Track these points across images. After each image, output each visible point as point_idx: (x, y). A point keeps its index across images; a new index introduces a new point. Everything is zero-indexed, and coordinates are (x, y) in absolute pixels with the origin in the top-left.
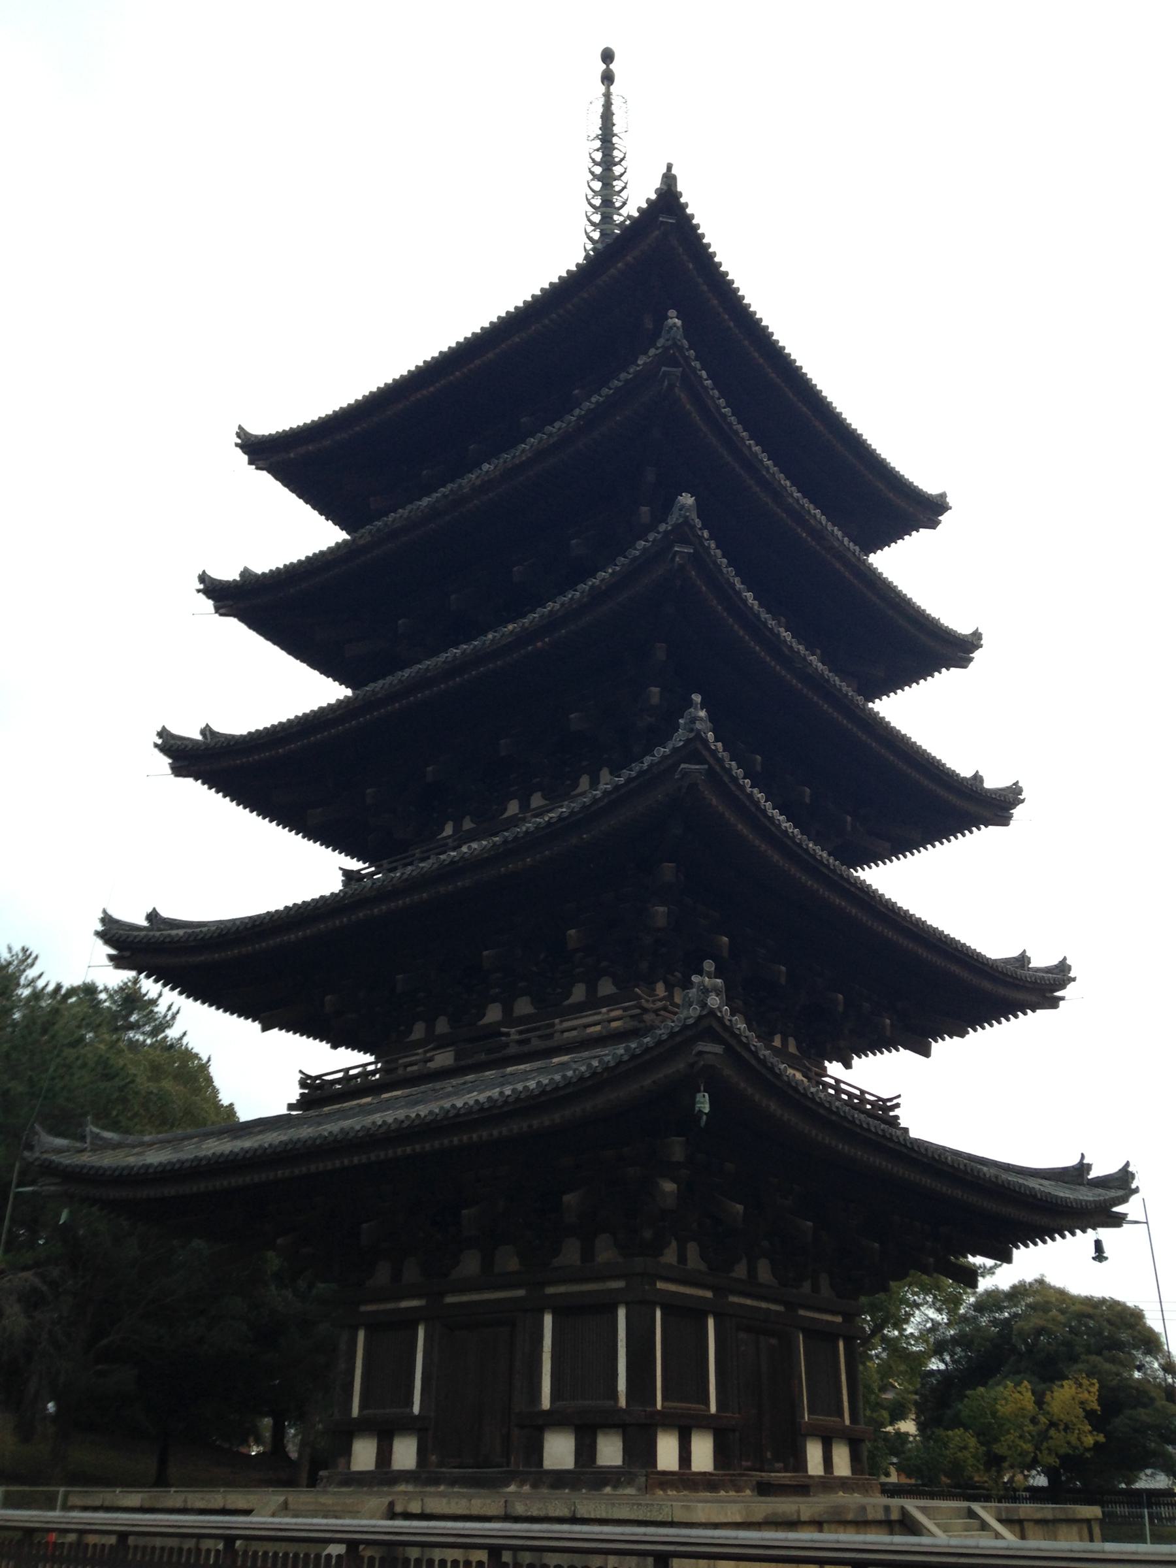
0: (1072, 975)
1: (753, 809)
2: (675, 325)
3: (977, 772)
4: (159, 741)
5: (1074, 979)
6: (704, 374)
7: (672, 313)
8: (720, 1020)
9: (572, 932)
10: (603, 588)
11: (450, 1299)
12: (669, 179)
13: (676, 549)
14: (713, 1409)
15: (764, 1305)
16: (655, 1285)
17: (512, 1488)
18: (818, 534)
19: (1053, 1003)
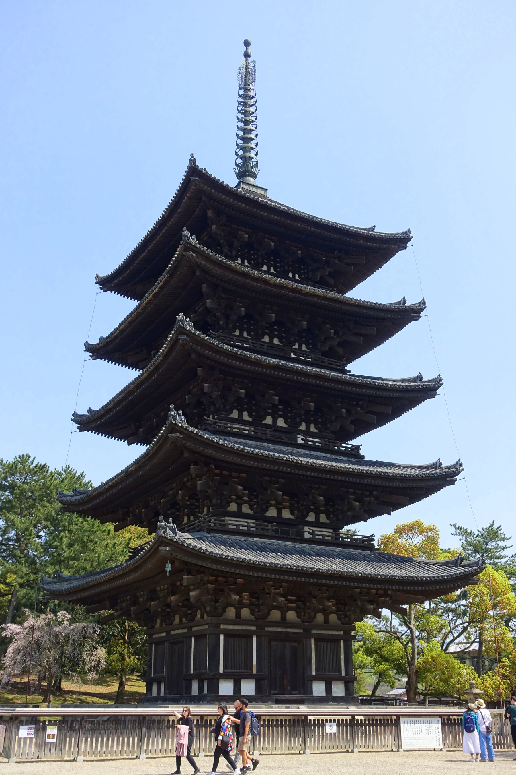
0: (461, 468)
1: (211, 443)
2: (185, 235)
3: (420, 373)
4: (73, 418)
5: (463, 470)
6: (205, 248)
7: (185, 229)
8: (165, 537)
9: (180, 492)
10: (165, 352)
11: (172, 633)
12: (192, 161)
13: (179, 338)
14: (254, 672)
15: (289, 630)
16: (220, 627)
17: (181, 702)
19: (452, 483)
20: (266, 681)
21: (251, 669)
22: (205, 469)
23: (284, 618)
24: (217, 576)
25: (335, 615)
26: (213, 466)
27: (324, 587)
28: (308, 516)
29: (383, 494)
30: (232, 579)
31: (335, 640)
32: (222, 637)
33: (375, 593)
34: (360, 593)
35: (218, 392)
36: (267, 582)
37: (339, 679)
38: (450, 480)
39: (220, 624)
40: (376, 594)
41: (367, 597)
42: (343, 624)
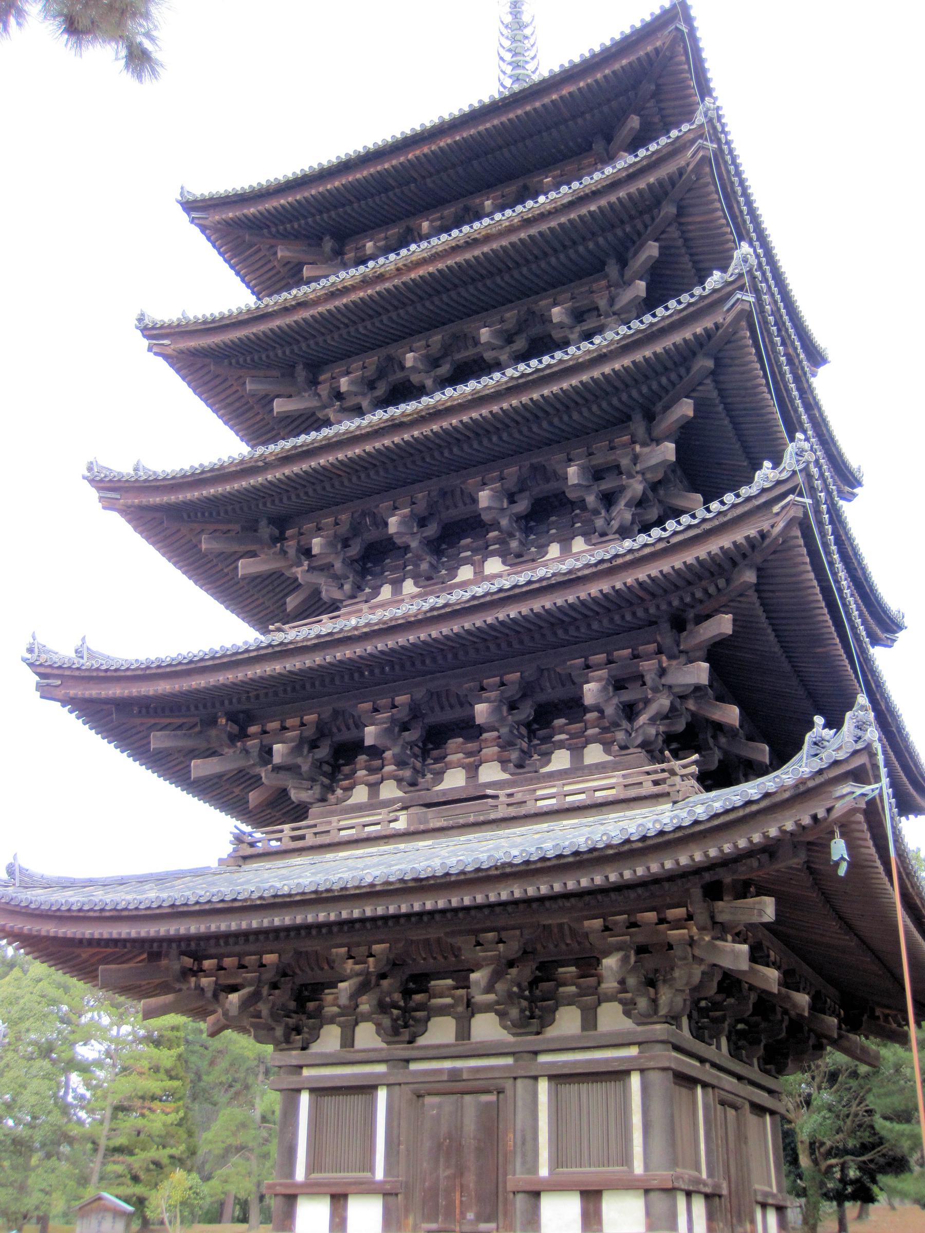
14: (379, 1175)
16: (300, 1073)
18: (365, 282)
20: (400, 1196)
21: (371, 1169)
22: (213, 732)
23: (464, 1032)
24: (220, 957)
25: (616, 1003)
26: (224, 721)
27: (491, 935)
28: (549, 762)
29: (685, 633)
30: (253, 957)
31: (619, 1075)
32: (305, 1098)
33: (656, 921)
34: (606, 929)
35: (300, 564)
36: (334, 950)
37: (627, 1185)
38: (783, 508)
39: (301, 1067)
40: (662, 921)
41: (628, 938)
42: (638, 1024)
